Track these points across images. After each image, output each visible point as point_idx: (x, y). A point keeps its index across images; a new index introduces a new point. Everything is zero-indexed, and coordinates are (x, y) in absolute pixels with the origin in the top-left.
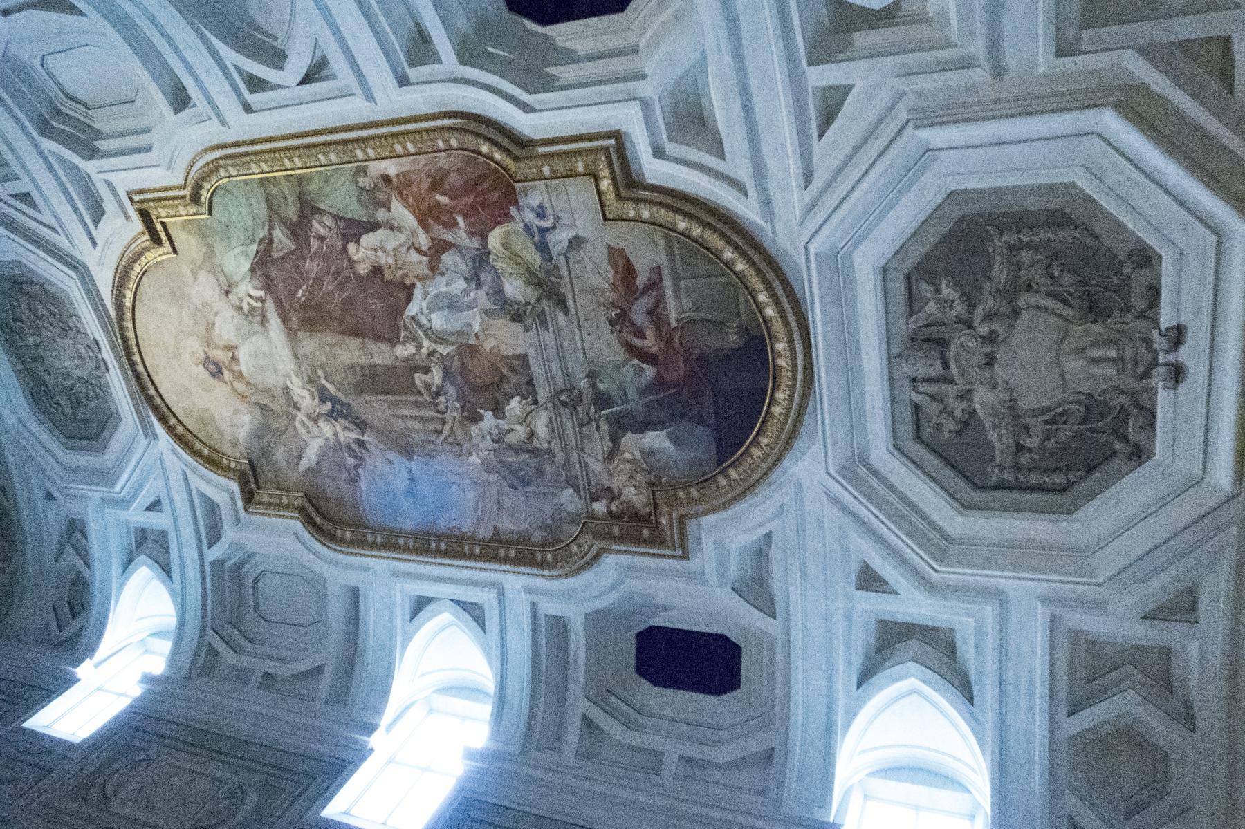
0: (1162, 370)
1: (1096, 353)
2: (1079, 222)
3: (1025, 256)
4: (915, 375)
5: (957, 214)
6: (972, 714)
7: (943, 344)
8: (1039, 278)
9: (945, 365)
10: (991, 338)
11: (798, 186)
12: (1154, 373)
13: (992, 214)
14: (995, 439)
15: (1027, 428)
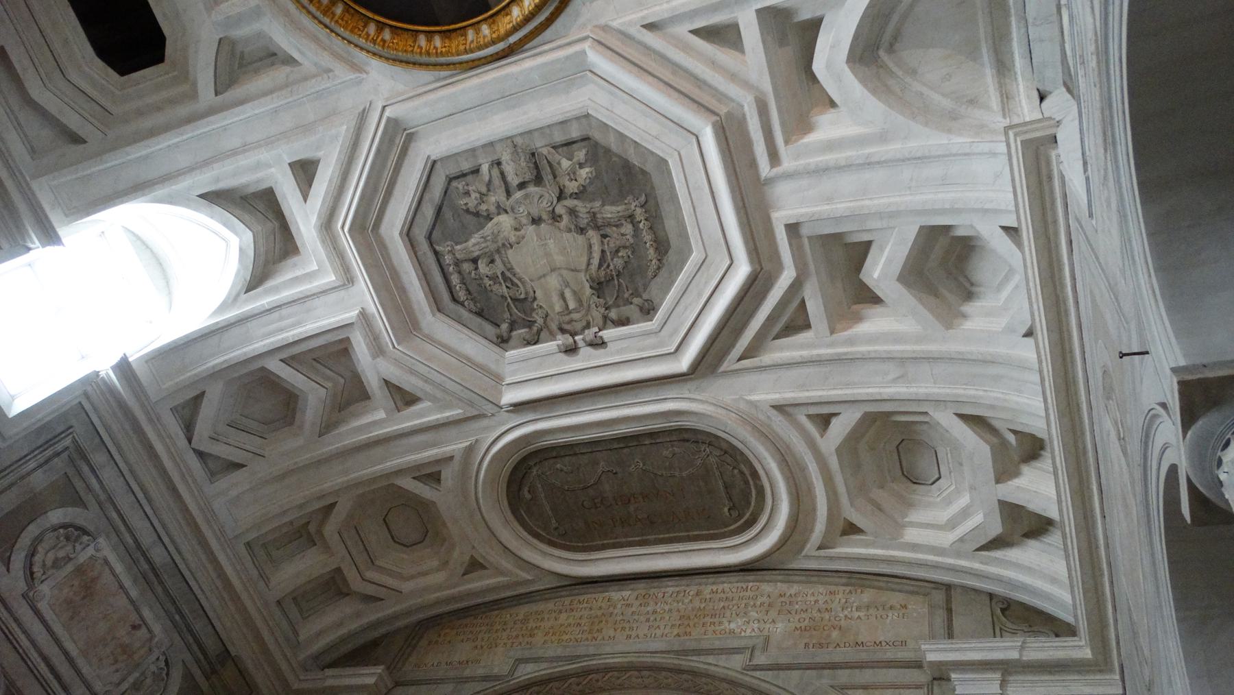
0: (571, 340)
1: (568, 294)
2: (664, 261)
3: (628, 229)
4: (504, 163)
5: (649, 168)
6: (238, 295)
7: (538, 180)
8: (612, 244)
9: (522, 186)
10: (556, 218)
11: (643, 18)
12: (567, 336)
13: (656, 198)
14: (473, 241)
15: (492, 261)
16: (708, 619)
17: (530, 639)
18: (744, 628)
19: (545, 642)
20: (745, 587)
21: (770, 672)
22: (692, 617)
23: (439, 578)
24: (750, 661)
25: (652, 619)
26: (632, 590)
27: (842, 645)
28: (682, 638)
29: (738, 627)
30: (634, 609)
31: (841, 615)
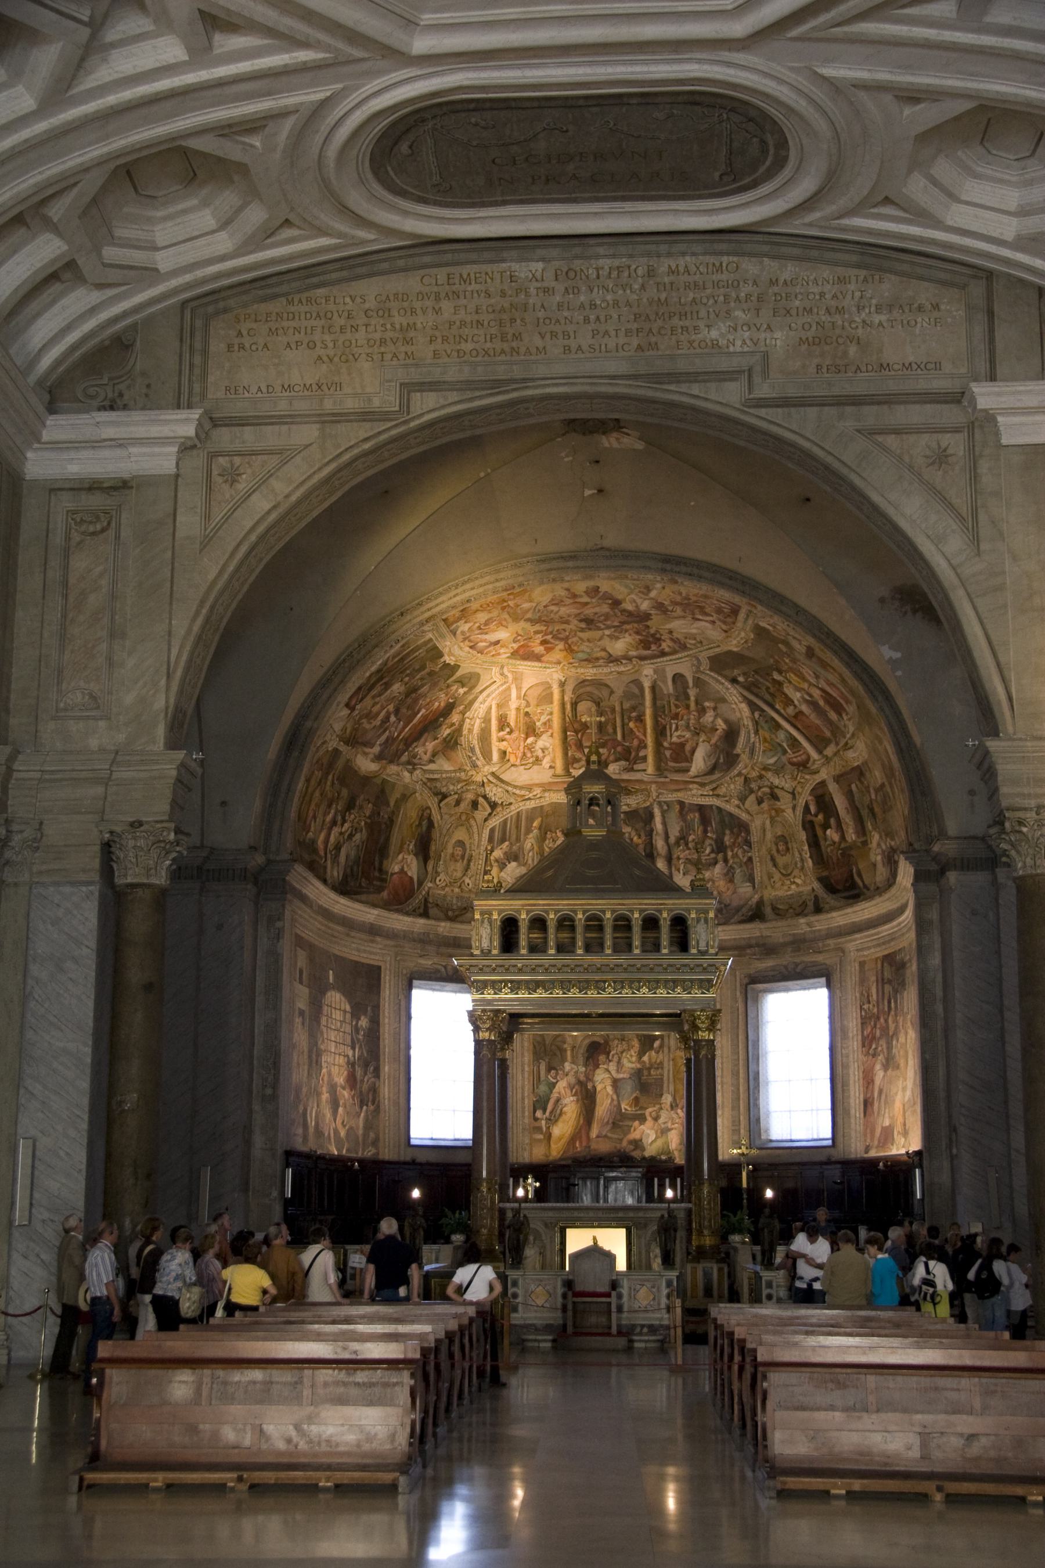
16: (675, 321)
17: (409, 349)
18: (731, 338)
19: (436, 354)
20: (718, 264)
21: (779, 410)
22: (653, 317)
23: (223, 242)
24: (750, 393)
25: (592, 317)
26: (543, 259)
27: (864, 369)
28: (648, 353)
29: (722, 335)
30: (558, 298)
31: (857, 319)
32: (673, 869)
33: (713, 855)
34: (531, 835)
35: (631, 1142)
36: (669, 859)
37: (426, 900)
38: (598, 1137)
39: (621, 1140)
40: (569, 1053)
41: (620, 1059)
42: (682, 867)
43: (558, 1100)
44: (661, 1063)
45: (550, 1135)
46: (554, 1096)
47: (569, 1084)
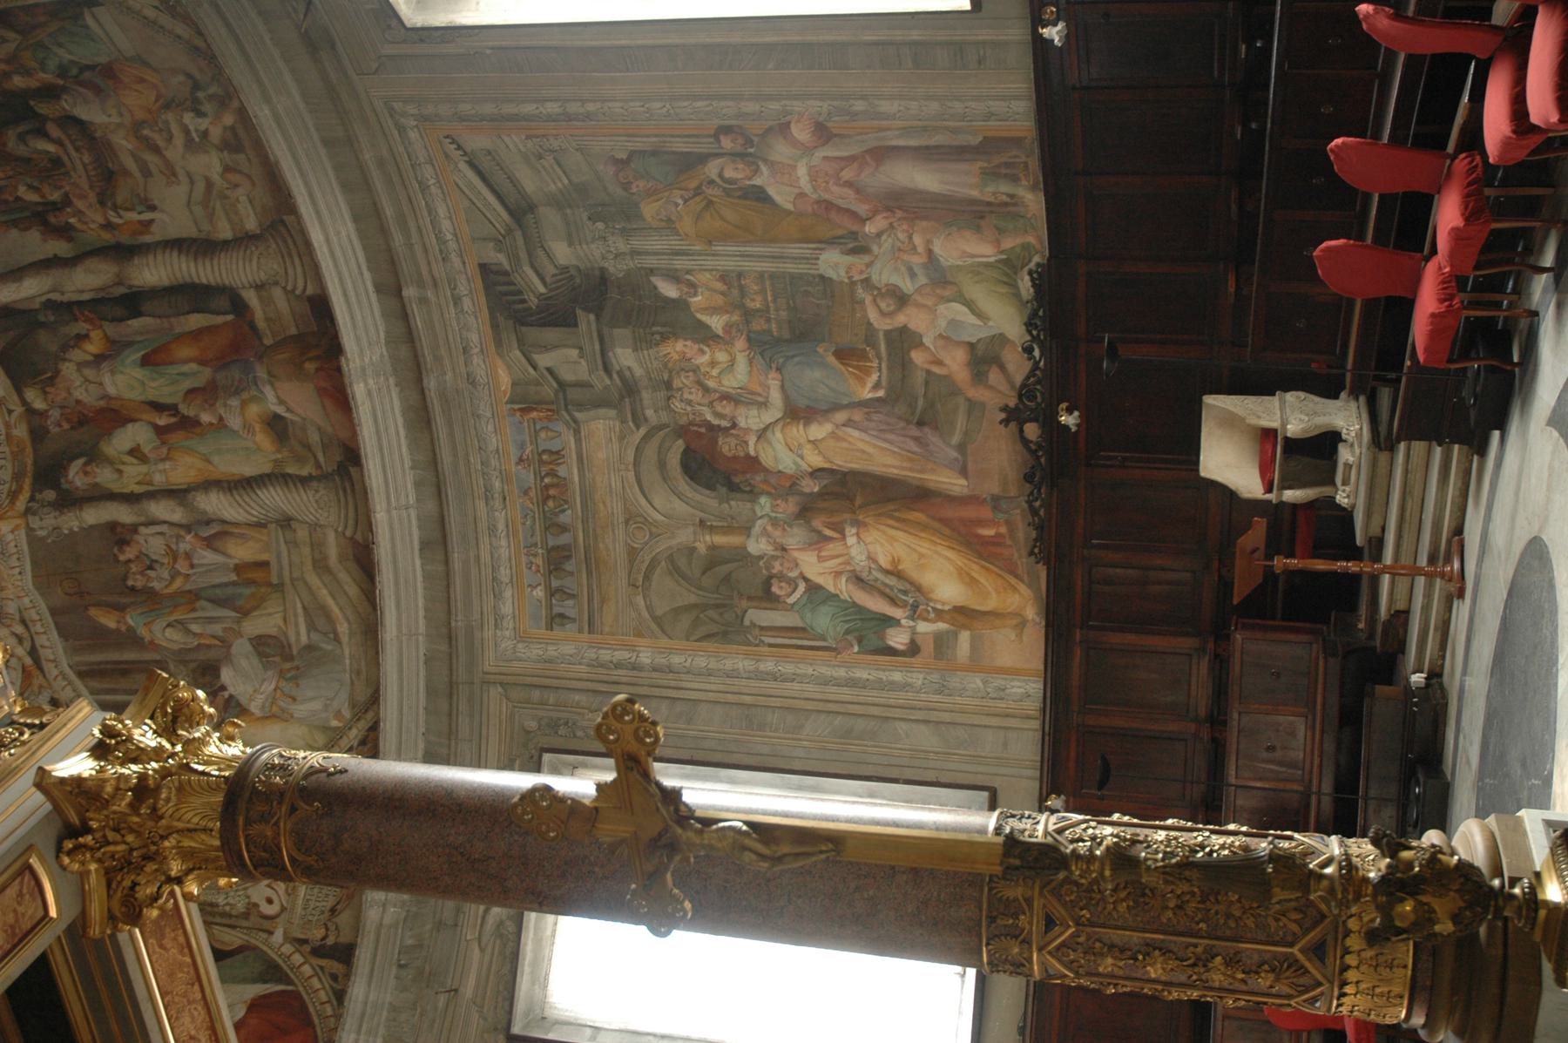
32: (147, 239)
33: (54, 131)
34: (142, 631)
35: (979, 376)
36: (124, 252)
37: (318, 951)
38: (964, 472)
39: (973, 405)
40: (719, 539)
41: (726, 397)
42: (133, 216)
43: (858, 580)
44: (724, 278)
45: (960, 610)
46: (844, 589)
47: (809, 546)
